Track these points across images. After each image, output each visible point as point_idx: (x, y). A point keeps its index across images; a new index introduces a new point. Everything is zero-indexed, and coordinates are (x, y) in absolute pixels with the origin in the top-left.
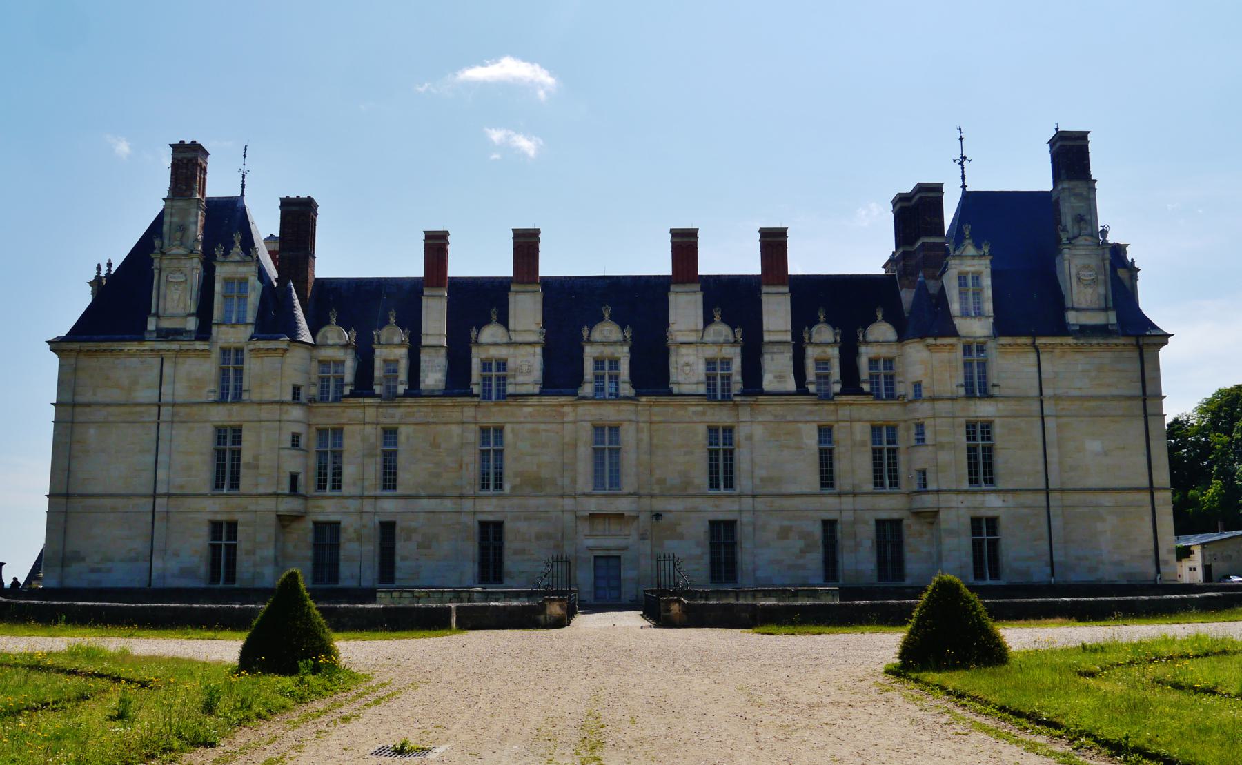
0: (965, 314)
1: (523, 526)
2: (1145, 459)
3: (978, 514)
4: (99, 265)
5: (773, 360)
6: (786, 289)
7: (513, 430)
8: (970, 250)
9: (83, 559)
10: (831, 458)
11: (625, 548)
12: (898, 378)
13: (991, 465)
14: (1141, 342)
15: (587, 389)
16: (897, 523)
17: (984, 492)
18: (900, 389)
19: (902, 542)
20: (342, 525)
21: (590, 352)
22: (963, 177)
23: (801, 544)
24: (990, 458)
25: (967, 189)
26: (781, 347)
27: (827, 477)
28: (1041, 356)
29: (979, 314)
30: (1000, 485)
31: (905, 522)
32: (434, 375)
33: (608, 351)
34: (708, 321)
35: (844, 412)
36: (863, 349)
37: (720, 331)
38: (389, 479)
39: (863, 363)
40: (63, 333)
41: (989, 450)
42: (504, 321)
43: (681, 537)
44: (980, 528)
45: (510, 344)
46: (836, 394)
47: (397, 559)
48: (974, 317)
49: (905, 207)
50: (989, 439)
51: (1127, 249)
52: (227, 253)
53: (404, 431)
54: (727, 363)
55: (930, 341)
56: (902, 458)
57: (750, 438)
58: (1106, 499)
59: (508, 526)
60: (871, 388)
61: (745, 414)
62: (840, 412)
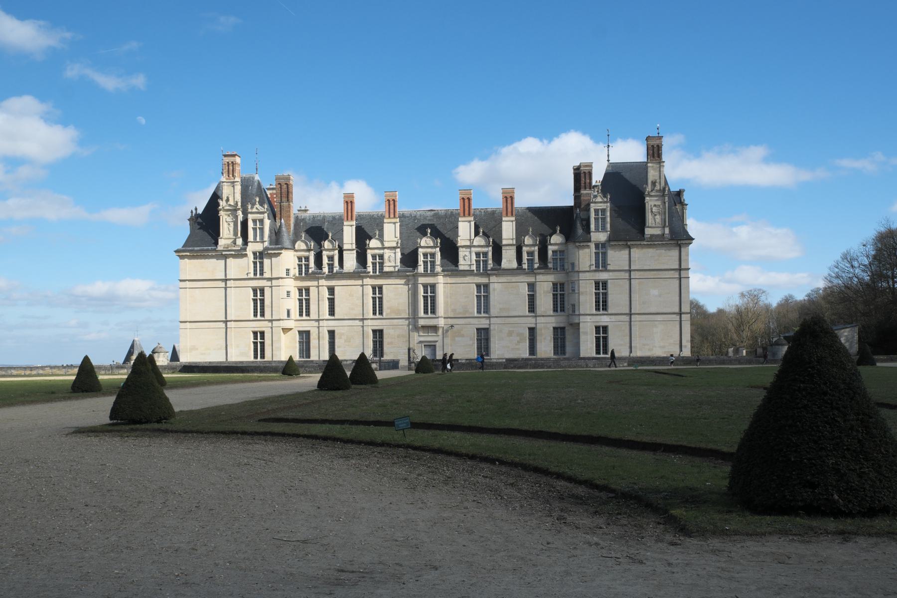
0: (597, 230)
1: (392, 332)
2: (677, 298)
3: (598, 324)
4: (192, 211)
5: (506, 252)
6: (513, 219)
7: (386, 288)
8: (599, 199)
9: (197, 349)
10: (533, 299)
11: (437, 341)
12: (566, 261)
13: (606, 302)
14: (679, 242)
15: (421, 269)
16: (563, 329)
17: (601, 315)
18: (566, 267)
19: (565, 337)
20: (311, 332)
21: (421, 251)
22: (608, 156)
23: (518, 338)
24: (606, 298)
25: (610, 162)
26: (511, 247)
27: (532, 308)
28: (631, 250)
29: (604, 229)
30: (610, 311)
31: (566, 328)
32: (350, 262)
33: (429, 250)
34: (477, 234)
35: (540, 278)
36: (550, 247)
37: (479, 241)
38: (332, 312)
39: (550, 253)
40: (180, 247)
41: (605, 295)
42: (381, 238)
43: (463, 336)
44: (599, 331)
45: (383, 248)
46: (536, 269)
47: (336, 347)
48: (601, 232)
49: (576, 173)
50: (605, 289)
51: (684, 193)
52: (252, 208)
53: (337, 290)
54: (485, 254)
55: (577, 244)
56: (566, 299)
57: (494, 290)
58: (659, 317)
59: (385, 332)
60: (553, 266)
61: (493, 279)
62: (537, 277)
